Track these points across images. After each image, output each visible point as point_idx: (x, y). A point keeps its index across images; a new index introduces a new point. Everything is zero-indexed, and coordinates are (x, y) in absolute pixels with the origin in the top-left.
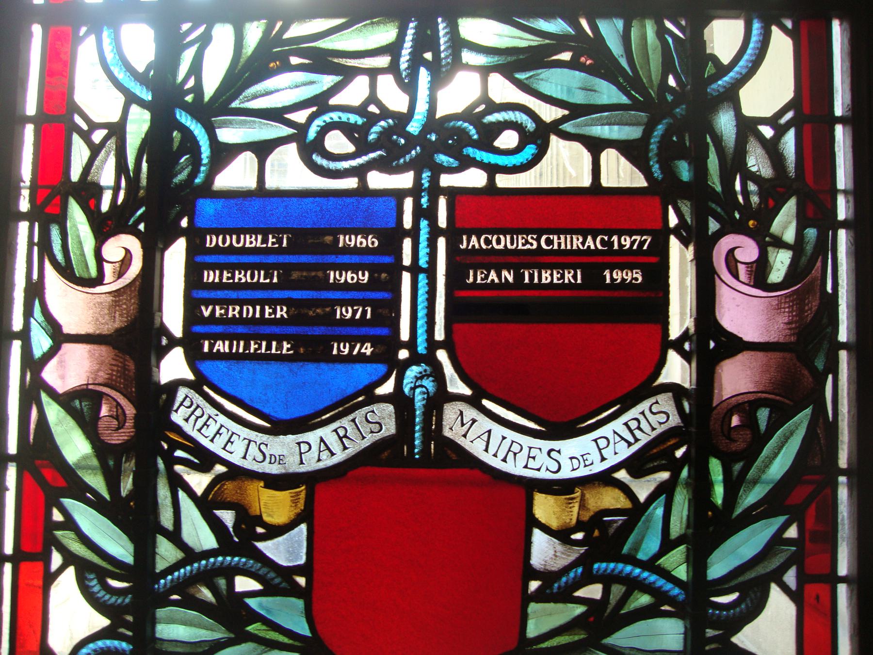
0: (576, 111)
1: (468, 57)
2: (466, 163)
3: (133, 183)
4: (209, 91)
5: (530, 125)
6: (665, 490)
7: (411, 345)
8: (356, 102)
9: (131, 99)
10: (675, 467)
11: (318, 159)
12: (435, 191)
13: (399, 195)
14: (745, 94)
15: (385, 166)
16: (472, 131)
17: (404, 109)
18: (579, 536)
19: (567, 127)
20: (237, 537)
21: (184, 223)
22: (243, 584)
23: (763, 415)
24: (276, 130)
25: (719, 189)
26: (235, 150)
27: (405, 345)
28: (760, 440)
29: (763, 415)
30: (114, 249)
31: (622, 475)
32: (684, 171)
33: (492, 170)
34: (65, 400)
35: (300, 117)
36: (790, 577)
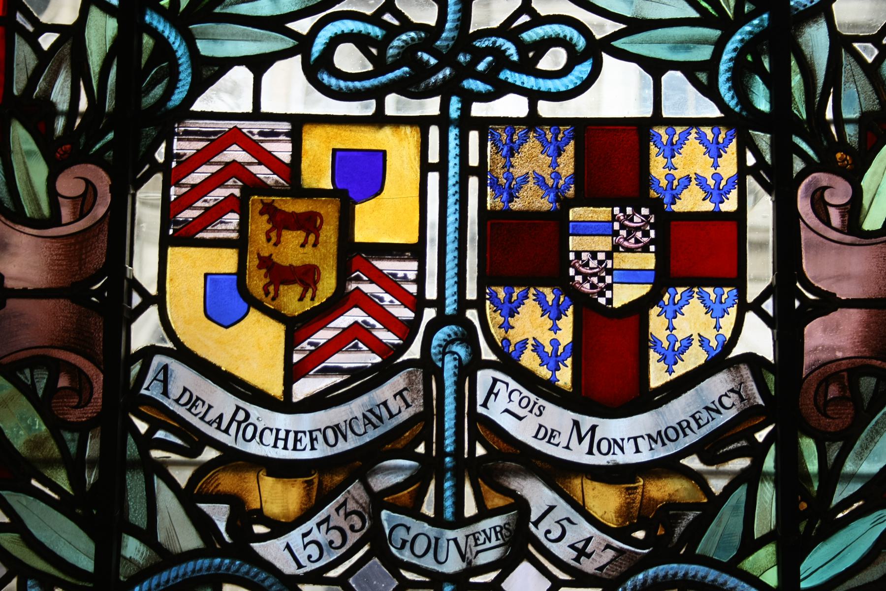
2: (502, 89)
5: (581, 43)
7: (439, 303)
11: (326, 78)
12: (467, 123)
13: (422, 123)
15: (405, 88)
16: (511, 50)
17: (433, 23)
18: (640, 535)
20: (219, 544)
24: (276, 42)
27: (431, 304)
33: (534, 96)
35: (303, 26)
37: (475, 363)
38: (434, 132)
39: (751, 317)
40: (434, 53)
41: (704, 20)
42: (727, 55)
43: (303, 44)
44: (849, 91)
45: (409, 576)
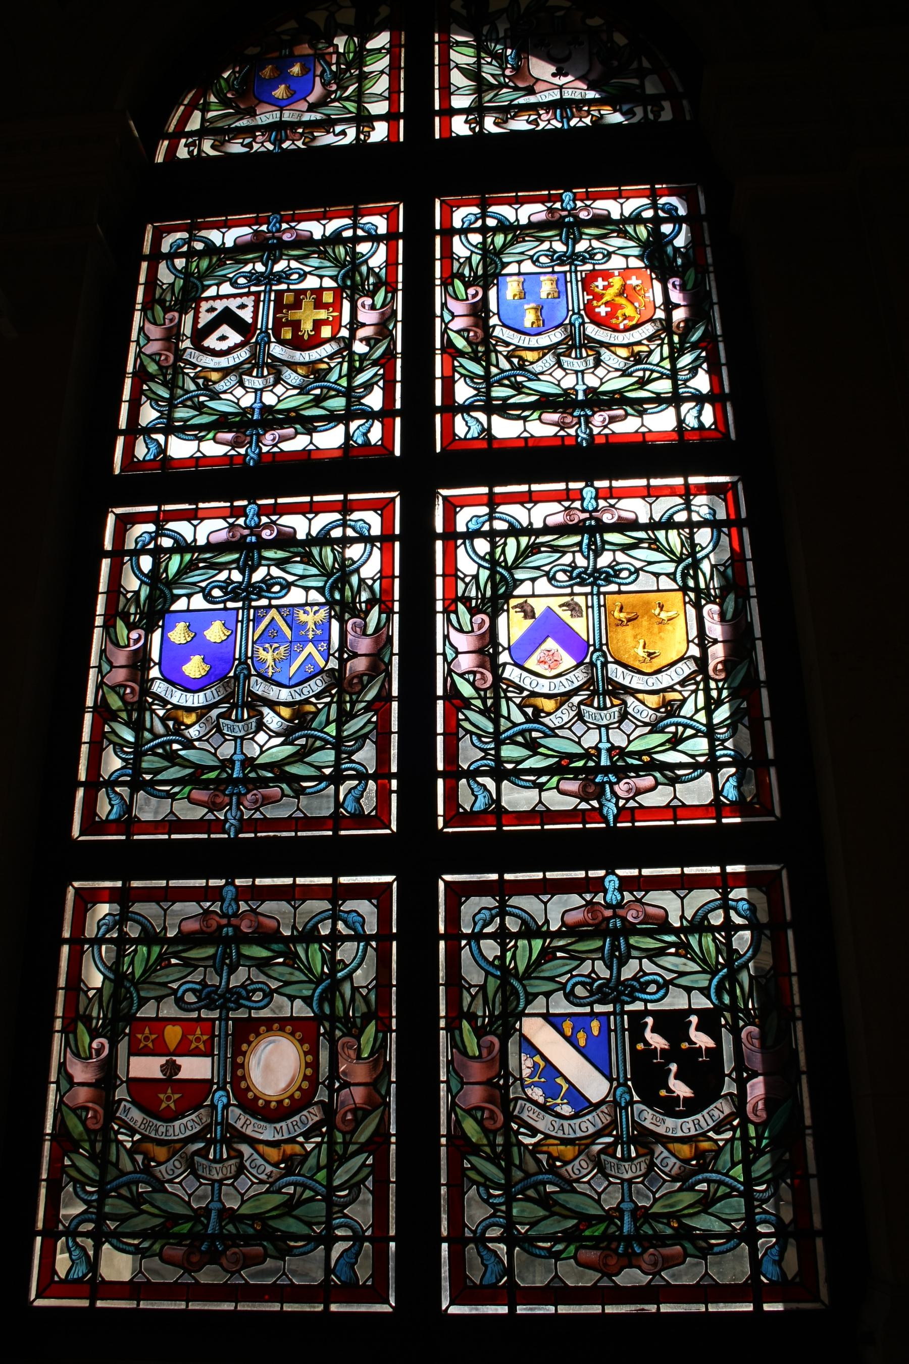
1: (263, 562)
2: (260, 597)
4: (170, 577)
6: (328, 705)
9: (142, 582)
10: (332, 696)
13: (237, 609)
14: (362, 570)
15: (233, 600)
19: (298, 583)
21: (160, 623)
22: (176, 746)
23: (365, 678)
26: (179, 597)
28: (364, 687)
29: (365, 678)
31: (313, 700)
32: (337, 596)
33: (270, 599)
37: (248, 677)
40: (241, 589)
42: (328, 584)
43: (203, 590)
45: (227, 737)
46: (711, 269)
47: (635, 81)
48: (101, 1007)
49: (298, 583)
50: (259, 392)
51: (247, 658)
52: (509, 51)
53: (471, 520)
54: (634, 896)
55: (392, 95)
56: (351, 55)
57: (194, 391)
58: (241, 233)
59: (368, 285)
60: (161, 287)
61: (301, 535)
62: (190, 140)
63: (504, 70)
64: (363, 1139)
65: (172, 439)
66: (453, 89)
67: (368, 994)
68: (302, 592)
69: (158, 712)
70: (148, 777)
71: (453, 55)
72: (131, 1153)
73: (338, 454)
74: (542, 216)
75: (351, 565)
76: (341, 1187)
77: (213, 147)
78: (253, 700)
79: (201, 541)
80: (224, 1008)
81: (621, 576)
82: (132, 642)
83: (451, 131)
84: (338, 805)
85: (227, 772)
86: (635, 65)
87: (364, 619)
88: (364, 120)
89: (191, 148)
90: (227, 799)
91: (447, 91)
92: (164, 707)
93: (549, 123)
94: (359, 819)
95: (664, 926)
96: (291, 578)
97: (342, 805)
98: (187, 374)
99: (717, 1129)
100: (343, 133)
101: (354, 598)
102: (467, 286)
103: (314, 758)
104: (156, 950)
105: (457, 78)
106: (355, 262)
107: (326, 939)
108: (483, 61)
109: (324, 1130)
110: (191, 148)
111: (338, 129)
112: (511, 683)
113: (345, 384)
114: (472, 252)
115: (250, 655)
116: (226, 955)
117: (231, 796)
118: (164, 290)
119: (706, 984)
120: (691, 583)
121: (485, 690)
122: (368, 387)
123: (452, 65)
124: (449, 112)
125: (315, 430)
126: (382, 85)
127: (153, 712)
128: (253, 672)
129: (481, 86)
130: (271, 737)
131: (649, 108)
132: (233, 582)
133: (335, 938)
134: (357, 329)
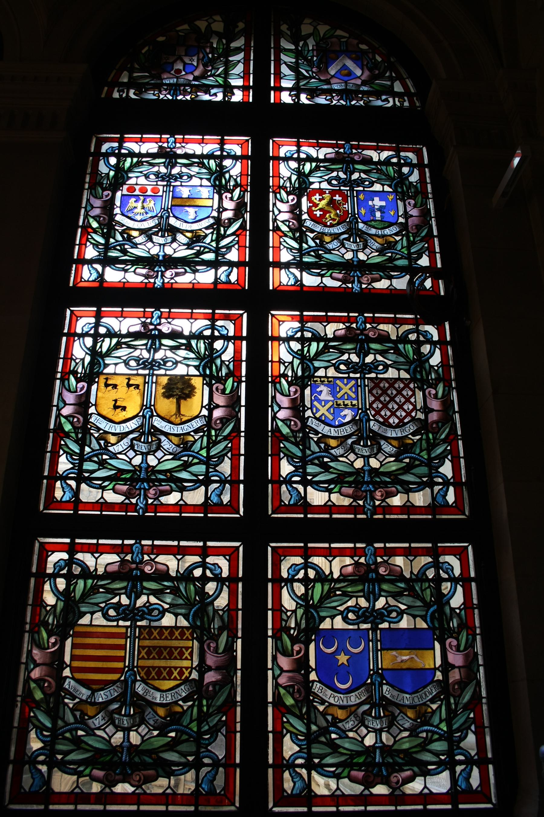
0: (185, 358)
1: (162, 347)
2: (160, 368)
3: (85, 371)
5: (174, 361)
8: (137, 355)
12: (153, 375)
15: (143, 369)
16: (162, 363)
25: (216, 375)
30: (80, 385)
31: (192, 433)
33: (166, 370)
34: (66, 417)
36: (229, 455)
38: (147, 377)
39: (204, 409)
41: (197, 358)
44: (223, 369)
45: (138, 453)
46: (430, 196)
47: (389, 83)
48: (55, 616)
49: (183, 362)
50: (162, 246)
51: (151, 405)
52: (315, 58)
53: (289, 330)
54: (383, 559)
55: (245, 76)
56: (221, 50)
57: (121, 241)
58: (152, 147)
59: (230, 186)
60: (101, 175)
61: (186, 333)
62: (121, 88)
63: (312, 68)
64: (219, 703)
65: (108, 269)
66: (282, 75)
67: (223, 614)
68: (186, 367)
69: (95, 434)
70: (86, 475)
71: (283, 57)
72: (72, 710)
73: (212, 287)
74: (333, 156)
75: (215, 353)
76: (206, 733)
77: (134, 94)
78: (155, 431)
79: (124, 332)
80: (134, 621)
81: (379, 369)
82: (79, 390)
83: (281, 100)
84: (207, 498)
85: (137, 474)
86: (387, 74)
87: (224, 385)
88: (228, 89)
89: (121, 93)
90: (138, 492)
91: (279, 76)
92: (98, 431)
93: (338, 102)
94: (220, 507)
95: (401, 577)
96: (179, 359)
97: (210, 498)
98: (117, 230)
99: (433, 701)
100: (215, 95)
101: (218, 373)
102: (288, 194)
103: (193, 469)
104: (90, 582)
105: (284, 69)
106: (221, 171)
107: (198, 579)
108: (300, 61)
109: (195, 697)
110: (121, 93)
111: (213, 91)
112: (312, 429)
113: (215, 245)
114: (292, 173)
115: (152, 403)
116: (134, 586)
117: (140, 489)
118: (102, 177)
119: (424, 613)
120: (419, 377)
121: (297, 432)
122: (229, 248)
123: (282, 62)
124: (279, 89)
125: (197, 271)
126: (240, 68)
127: (92, 434)
128: (155, 414)
129: (299, 77)
130: (165, 455)
131: (397, 99)
132: (143, 358)
133: (204, 579)
134: (222, 212)
